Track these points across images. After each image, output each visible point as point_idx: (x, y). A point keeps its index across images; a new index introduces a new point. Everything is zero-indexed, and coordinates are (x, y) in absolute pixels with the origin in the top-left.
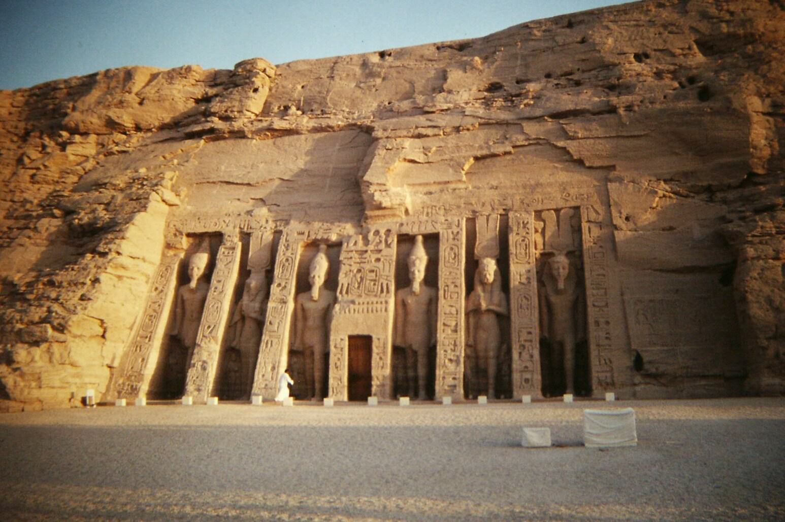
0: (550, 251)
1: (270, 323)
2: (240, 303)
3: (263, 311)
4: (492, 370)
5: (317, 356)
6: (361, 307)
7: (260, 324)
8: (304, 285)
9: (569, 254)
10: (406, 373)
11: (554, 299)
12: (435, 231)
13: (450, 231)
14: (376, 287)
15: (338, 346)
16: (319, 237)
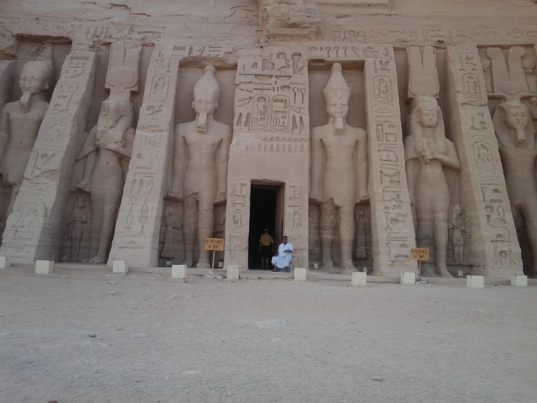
0: (500, 94)
1: (139, 155)
2: (93, 130)
3: (126, 142)
4: (442, 239)
5: (205, 207)
6: (269, 144)
7: (123, 160)
8: (184, 112)
9: (525, 99)
10: (320, 234)
11: (512, 151)
12: (360, 59)
13: (378, 62)
14: (286, 121)
15: (238, 193)
16: (205, 54)
